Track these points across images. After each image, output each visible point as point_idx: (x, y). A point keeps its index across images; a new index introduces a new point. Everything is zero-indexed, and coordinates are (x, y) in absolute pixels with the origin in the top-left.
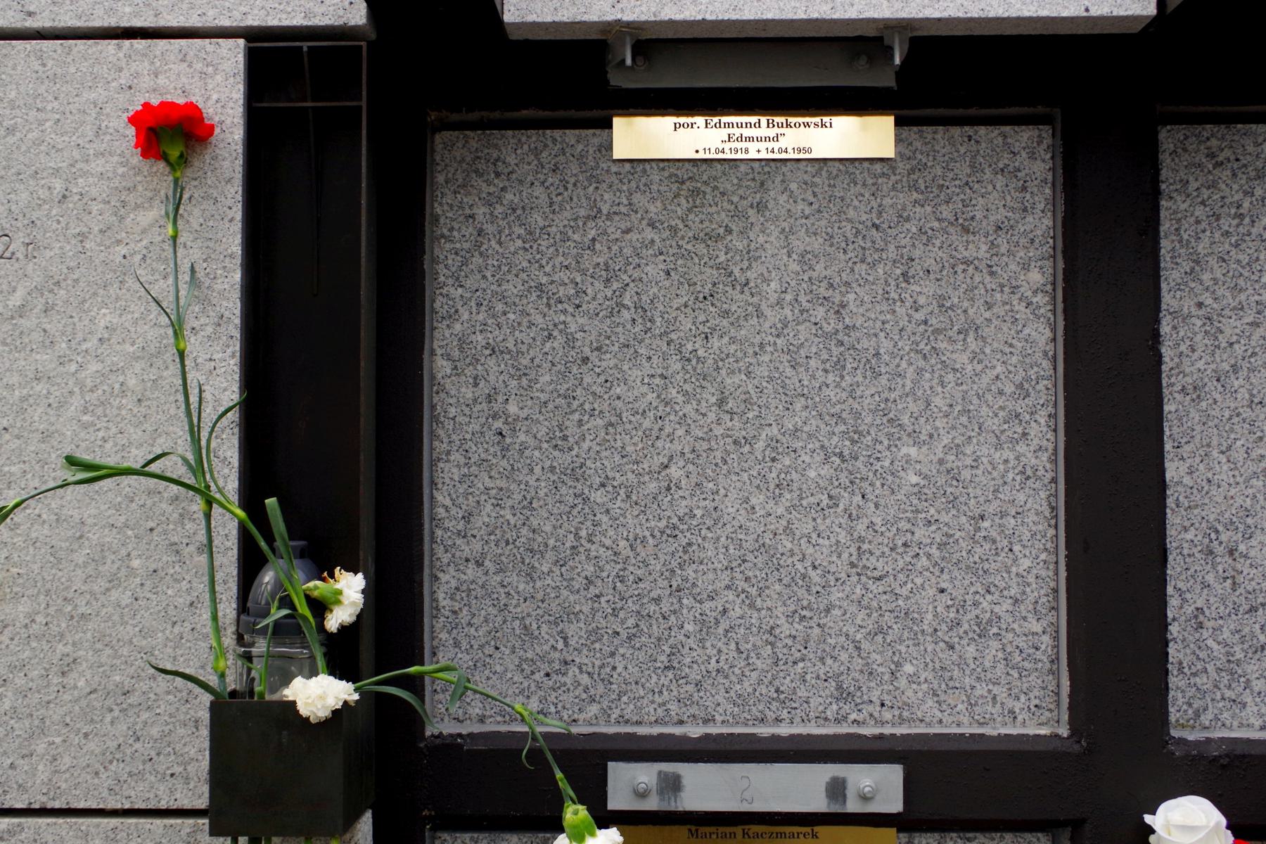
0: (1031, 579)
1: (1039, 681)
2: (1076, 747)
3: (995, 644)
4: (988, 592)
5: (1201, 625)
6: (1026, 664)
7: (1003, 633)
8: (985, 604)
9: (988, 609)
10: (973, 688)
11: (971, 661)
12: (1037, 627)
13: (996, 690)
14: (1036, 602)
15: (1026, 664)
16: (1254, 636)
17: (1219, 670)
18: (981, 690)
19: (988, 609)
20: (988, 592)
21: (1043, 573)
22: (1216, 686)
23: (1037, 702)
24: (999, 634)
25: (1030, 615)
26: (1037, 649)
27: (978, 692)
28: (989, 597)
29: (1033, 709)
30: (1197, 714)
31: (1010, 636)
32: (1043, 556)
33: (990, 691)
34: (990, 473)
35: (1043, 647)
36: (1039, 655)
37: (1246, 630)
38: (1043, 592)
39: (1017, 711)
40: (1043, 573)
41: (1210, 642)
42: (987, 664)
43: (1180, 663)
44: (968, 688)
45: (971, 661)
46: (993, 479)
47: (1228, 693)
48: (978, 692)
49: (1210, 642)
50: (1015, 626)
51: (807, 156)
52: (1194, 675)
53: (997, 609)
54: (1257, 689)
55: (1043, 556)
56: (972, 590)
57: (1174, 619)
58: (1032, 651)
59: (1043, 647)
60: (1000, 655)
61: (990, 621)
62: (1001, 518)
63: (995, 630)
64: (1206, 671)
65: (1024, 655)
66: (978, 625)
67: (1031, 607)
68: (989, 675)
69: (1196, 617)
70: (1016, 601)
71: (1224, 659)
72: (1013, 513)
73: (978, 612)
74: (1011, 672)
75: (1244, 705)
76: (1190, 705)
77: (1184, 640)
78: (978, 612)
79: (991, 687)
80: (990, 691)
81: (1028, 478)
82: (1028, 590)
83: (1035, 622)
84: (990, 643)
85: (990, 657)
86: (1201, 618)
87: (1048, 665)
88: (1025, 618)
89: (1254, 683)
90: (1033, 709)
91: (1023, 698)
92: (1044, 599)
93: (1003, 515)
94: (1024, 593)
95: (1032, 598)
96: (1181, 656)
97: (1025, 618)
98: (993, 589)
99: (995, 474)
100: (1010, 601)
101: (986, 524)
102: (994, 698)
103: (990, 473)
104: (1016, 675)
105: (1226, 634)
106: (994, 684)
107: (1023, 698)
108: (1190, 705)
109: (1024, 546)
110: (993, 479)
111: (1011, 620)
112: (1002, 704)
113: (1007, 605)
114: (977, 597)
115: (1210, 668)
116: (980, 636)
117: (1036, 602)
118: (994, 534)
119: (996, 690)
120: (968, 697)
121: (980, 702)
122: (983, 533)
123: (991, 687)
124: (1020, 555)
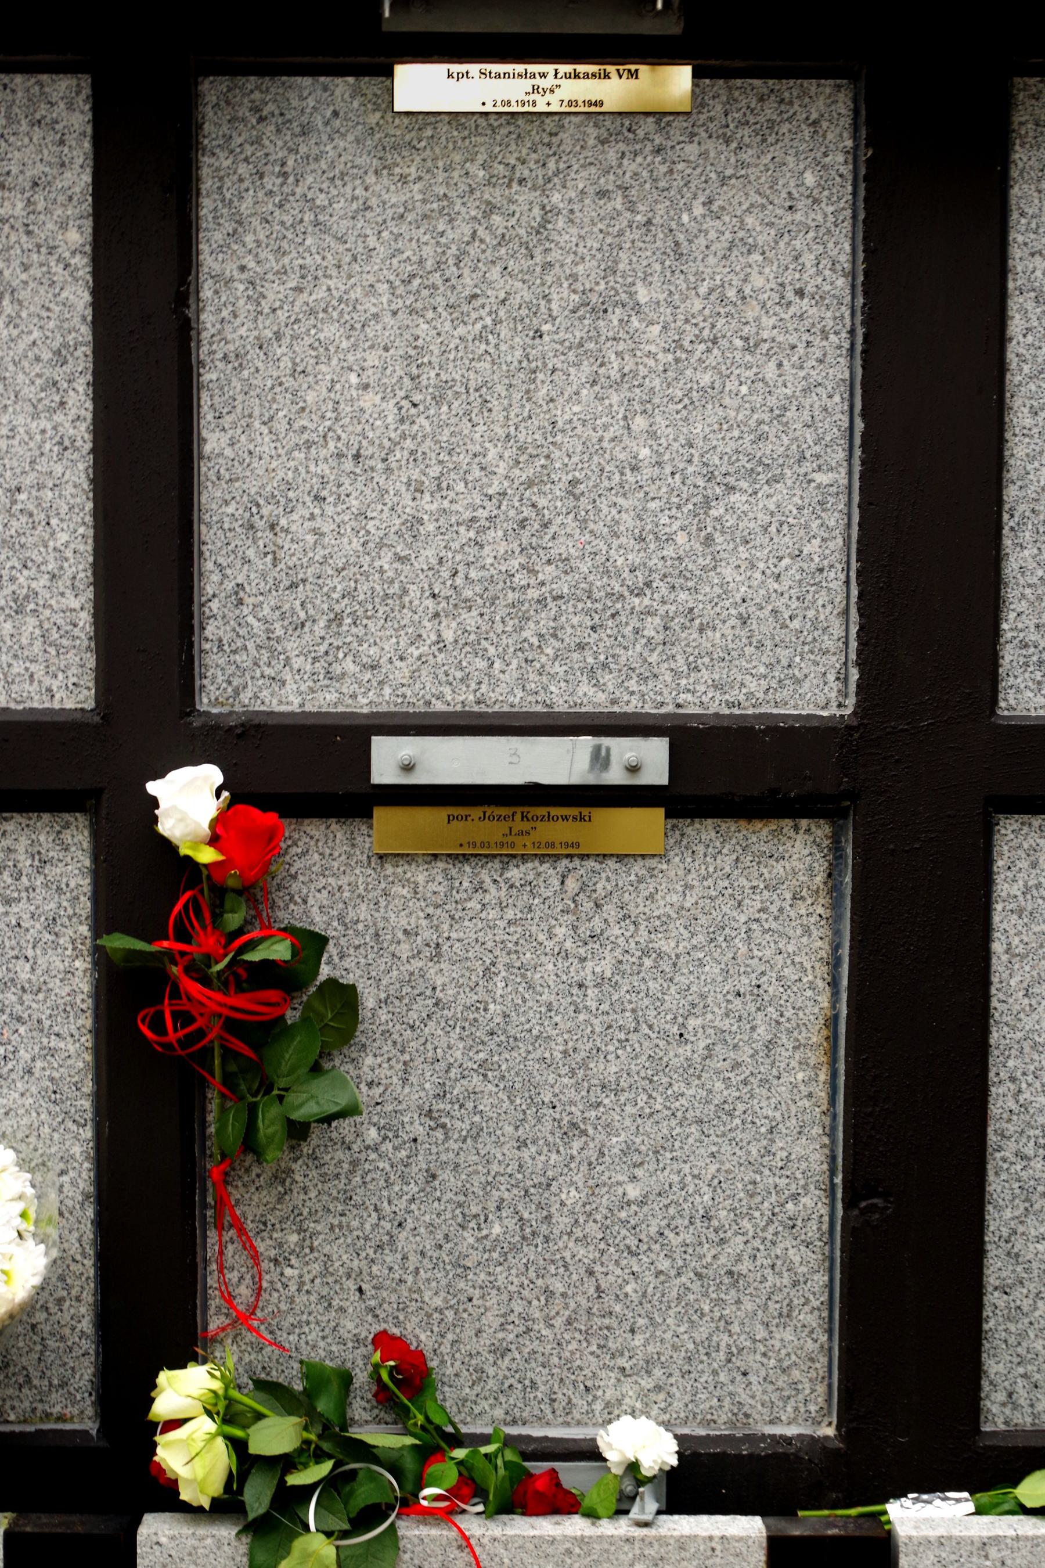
0: (69, 554)
1: (77, 659)
2: (97, 719)
3: (32, 621)
4: (25, 566)
5: (241, 602)
6: (64, 642)
7: (40, 609)
8: (22, 580)
9: (25, 584)
10: (10, 665)
11: (7, 639)
12: (75, 604)
13: (33, 668)
14: (74, 578)
15: (64, 642)
16: (293, 612)
17: (259, 647)
18: (18, 668)
19: (25, 584)
20: (25, 566)
21: (82, 548)
22: (255, 664)
23: (75, 680)
24: (35, 611)
25: (68, 592)
26: (75, 626)
27: (15, 670)
28: (25, 572)
29: (71, 687)
30: (237, 692)
31: (47, 612)
32: (81, 530)
33: (27, 669)
34: (26, 444)
35: (81, 624)
36: (76, 632)
37: (287, 606)
38: (81, 567)
39: (55, 689)
40: (82, 548)
41: (250, 619)
42: (25, 641)
43: (220, 640)
44: (5, 665)
45: (7, 639)
46: (30, 450)
47: (268, 671)
48: (15, 670)
49: (250, 619)
50: (53, 602)
51: (598, 109)
52: (234, 652)
53: (34, 585)
54: (296, 667)
55: (81, 530)
56: (9, 565)
57: (214, 596)
58: (69, 628)
59: (81, 624)
60: (37, 632)
61: (27, 597)
62: (39, 490)
63: (32, 606)
64: (246, 649)
65: (62, 632)
66: (15, 601)
67: (69, 583)
68: (26, 652)
69: (236, 593)
70: (54, 576)
71: (264, 636)
72: (51, 485)
73: (14, 587)
74: (49, 649)
75: (284, 683)
76: (230, 683)
77: (224, 617)
78: (14, 587)
79: (28, 664)
80: (27, 669)
81: (66, 449)
82: (66, 565)
83: (72, 598)
84: (28, 619)
85: (27, 634)
86: (241, 594)
87: (86, 643)
88: (62, 594)
89: (294, 660)
90: (71, 687)
91: (60, 676)
92: (82, 575)
93: (40, 487)
94: (61, 568)
95: (70, 572)
96: (221, 633)
97: (62, 594)
98: (29, 564)
99: (32, 444)
100: (47, 576)
101: (23, 496)
102: (32, 676)
103: (26, 444)
104: (54, 653)
105: (266, 611)
106: (31, 661)
107: (60, 676)
108: (230, 683)
109: (62, 520)
110: (30, 450)
111: (48, 596)
112: (40, 682)
113: (44, 580)
114: (14, 572)
115: (250, 645)
116: (17, 612)
117: (74, 578)
118: (31, 507)
119: (33, 668)
120: (5, 675)
121: (17, 680)
122: (19, 506)
123: (28, 664)
124: (58, 529)
